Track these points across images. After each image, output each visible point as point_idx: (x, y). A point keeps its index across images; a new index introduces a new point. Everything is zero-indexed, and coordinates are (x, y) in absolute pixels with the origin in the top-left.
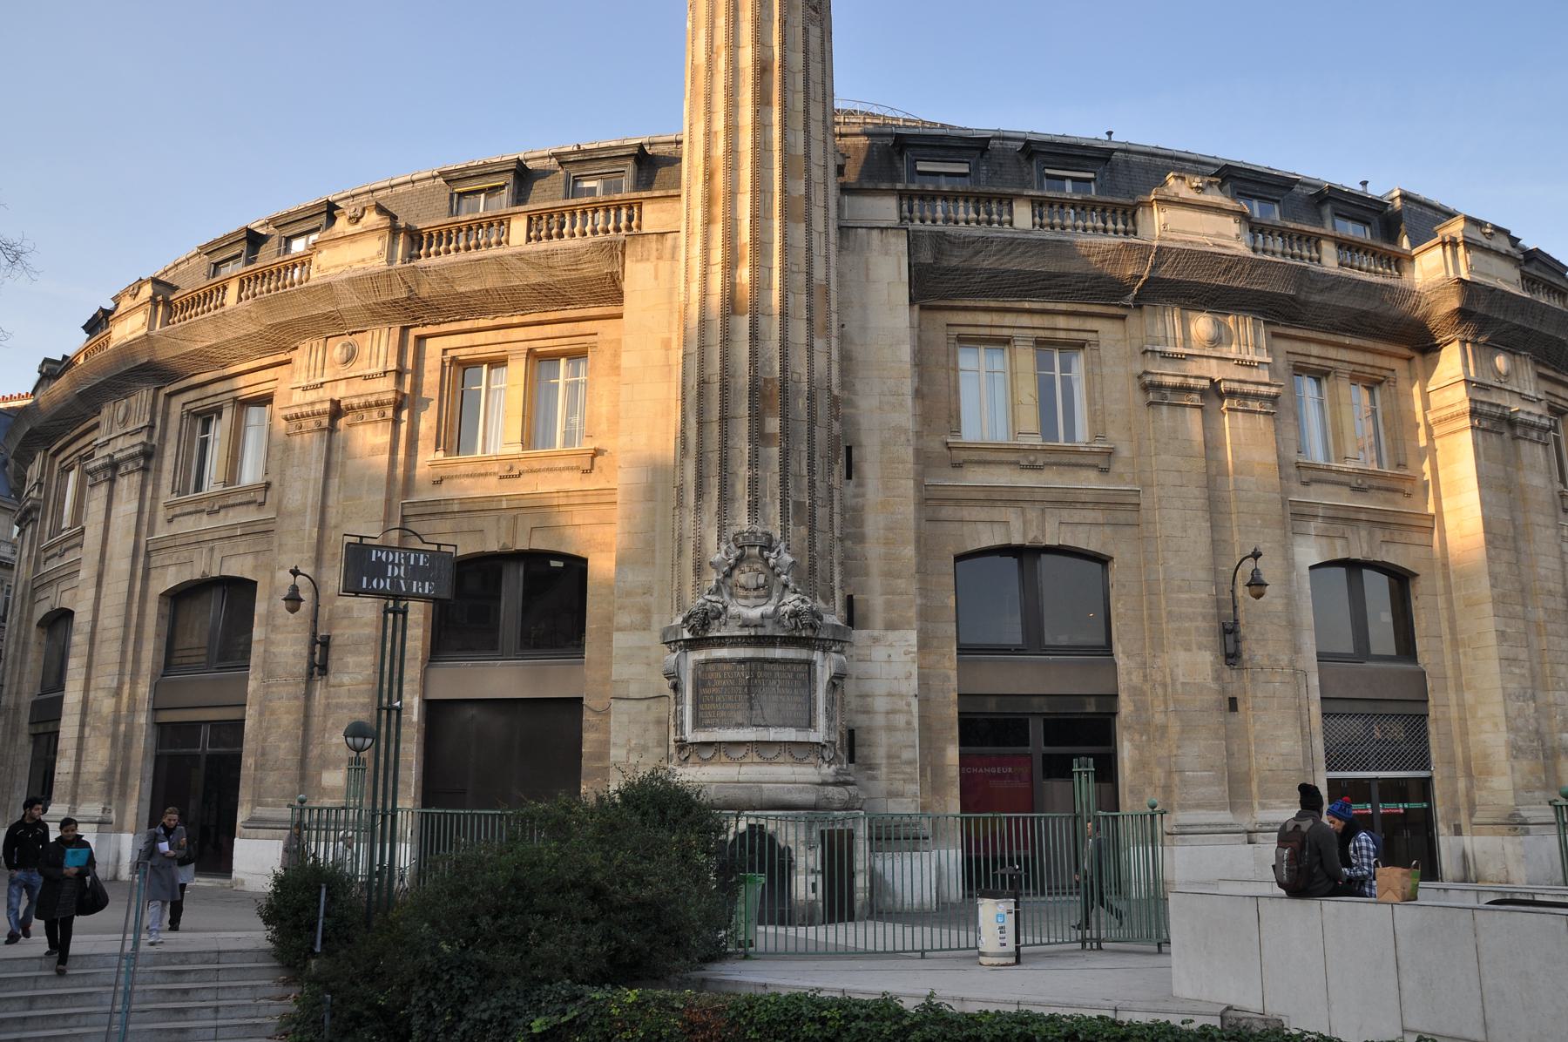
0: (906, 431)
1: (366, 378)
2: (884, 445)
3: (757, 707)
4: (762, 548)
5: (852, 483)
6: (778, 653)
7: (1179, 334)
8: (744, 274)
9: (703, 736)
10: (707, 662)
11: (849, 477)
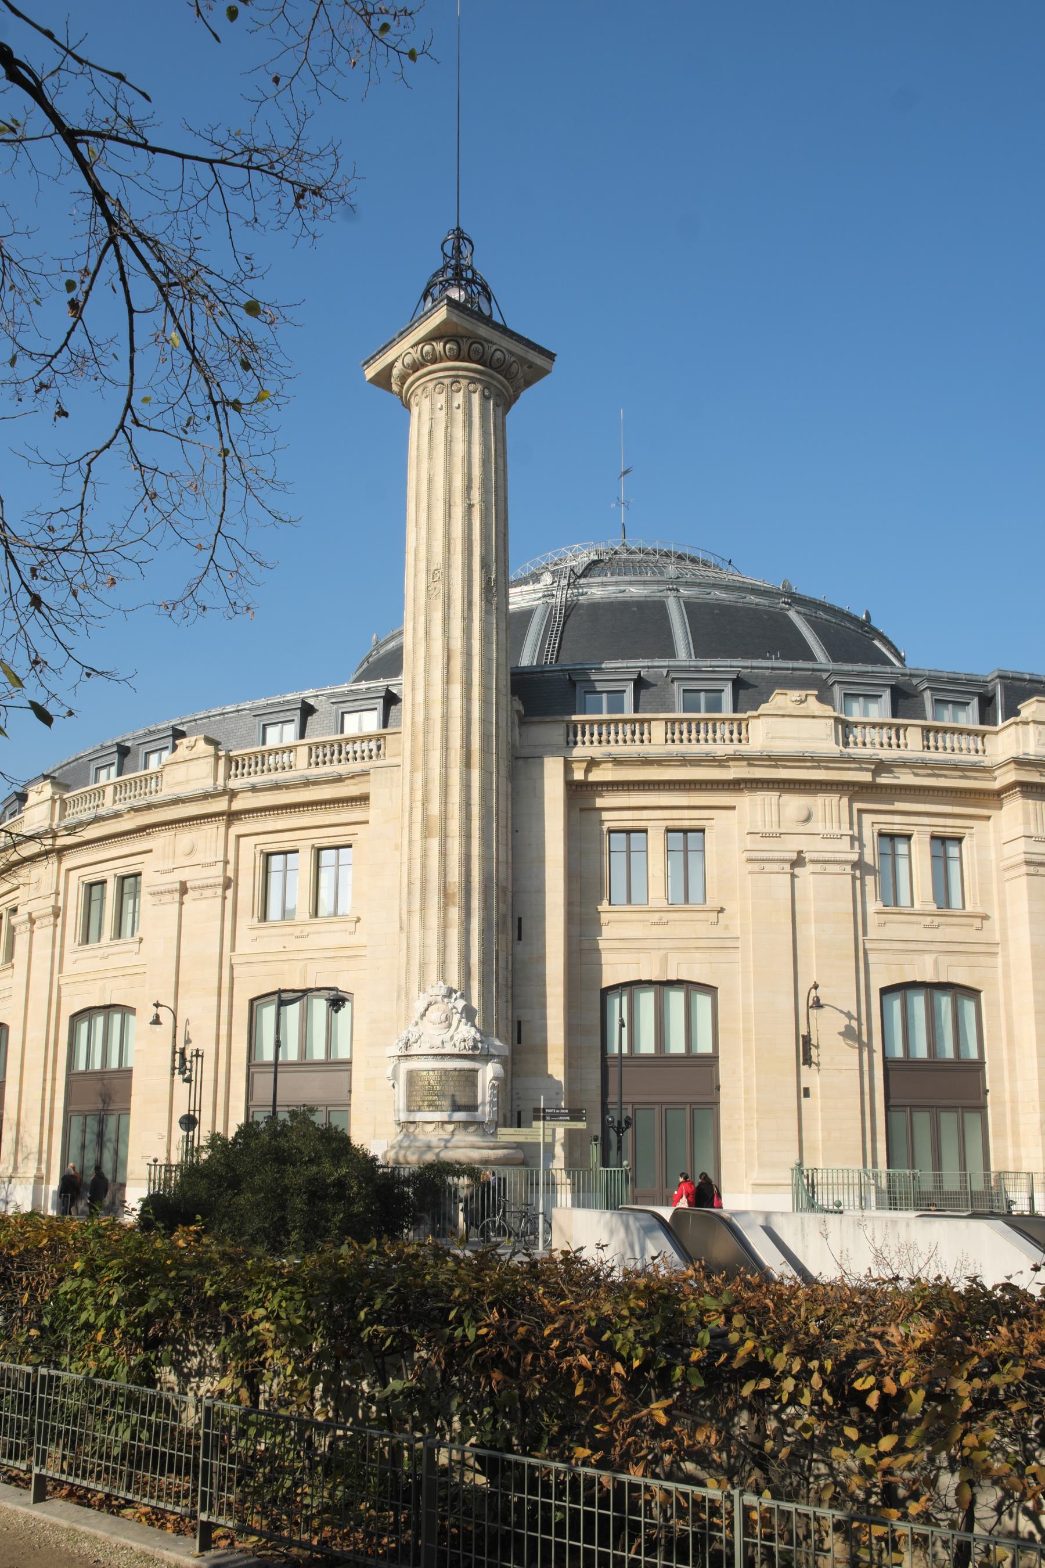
1: (205, 865)
5: (521, 942)
7: (775, 819)
8: (435, 809)
11: (520, 939)
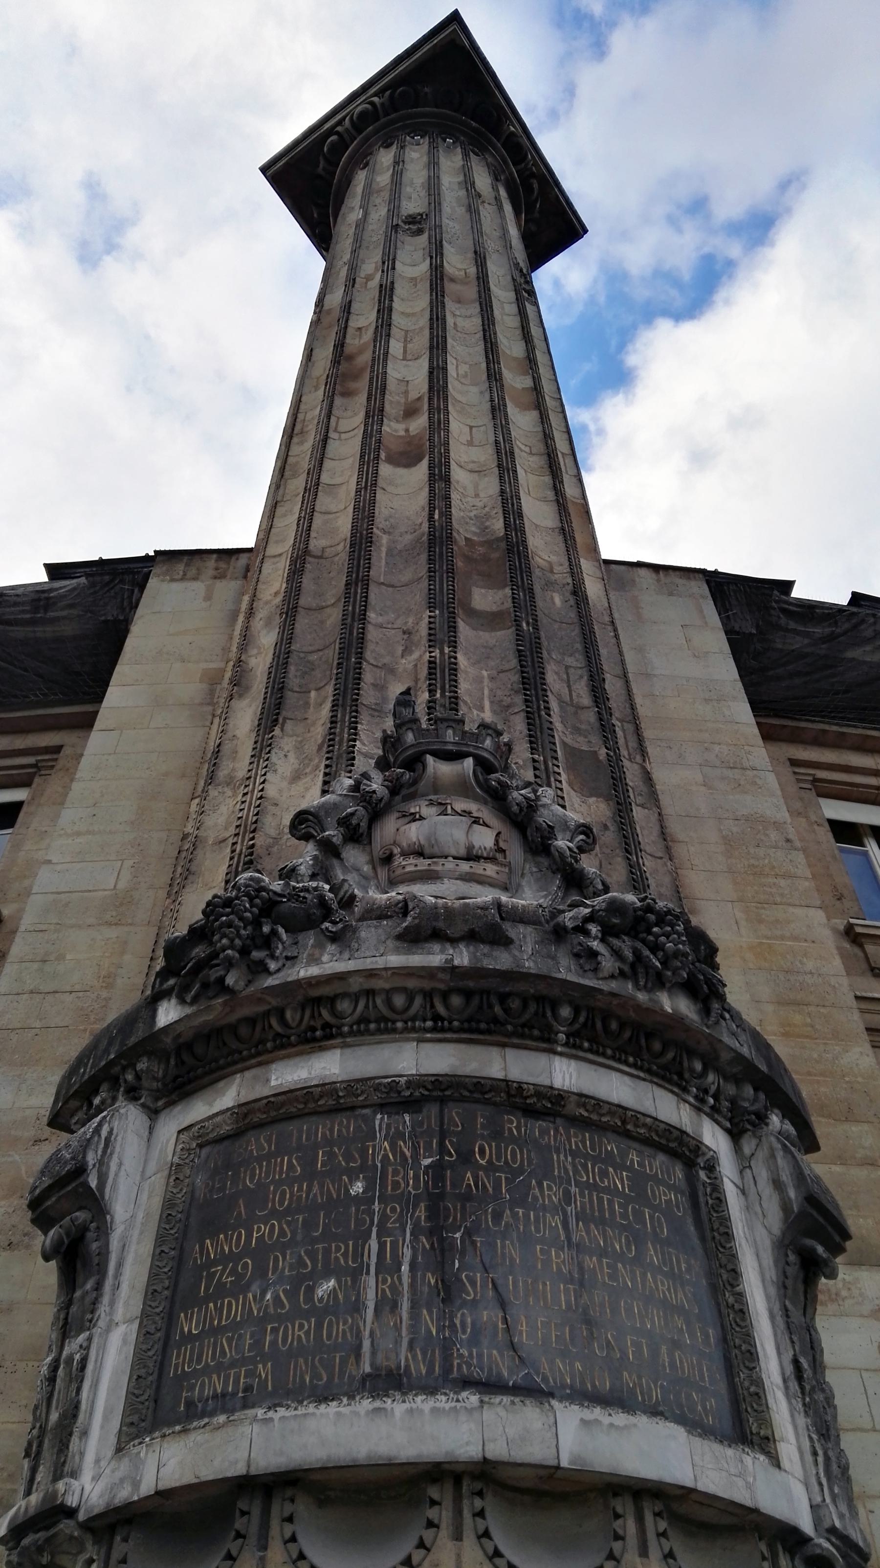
0: (778, 826)
2: (729, 843)
3: (474, 1285)
4: (484, 766)
6: (565, 1073)
9: (173, 1462)
10: (250, 1119)
